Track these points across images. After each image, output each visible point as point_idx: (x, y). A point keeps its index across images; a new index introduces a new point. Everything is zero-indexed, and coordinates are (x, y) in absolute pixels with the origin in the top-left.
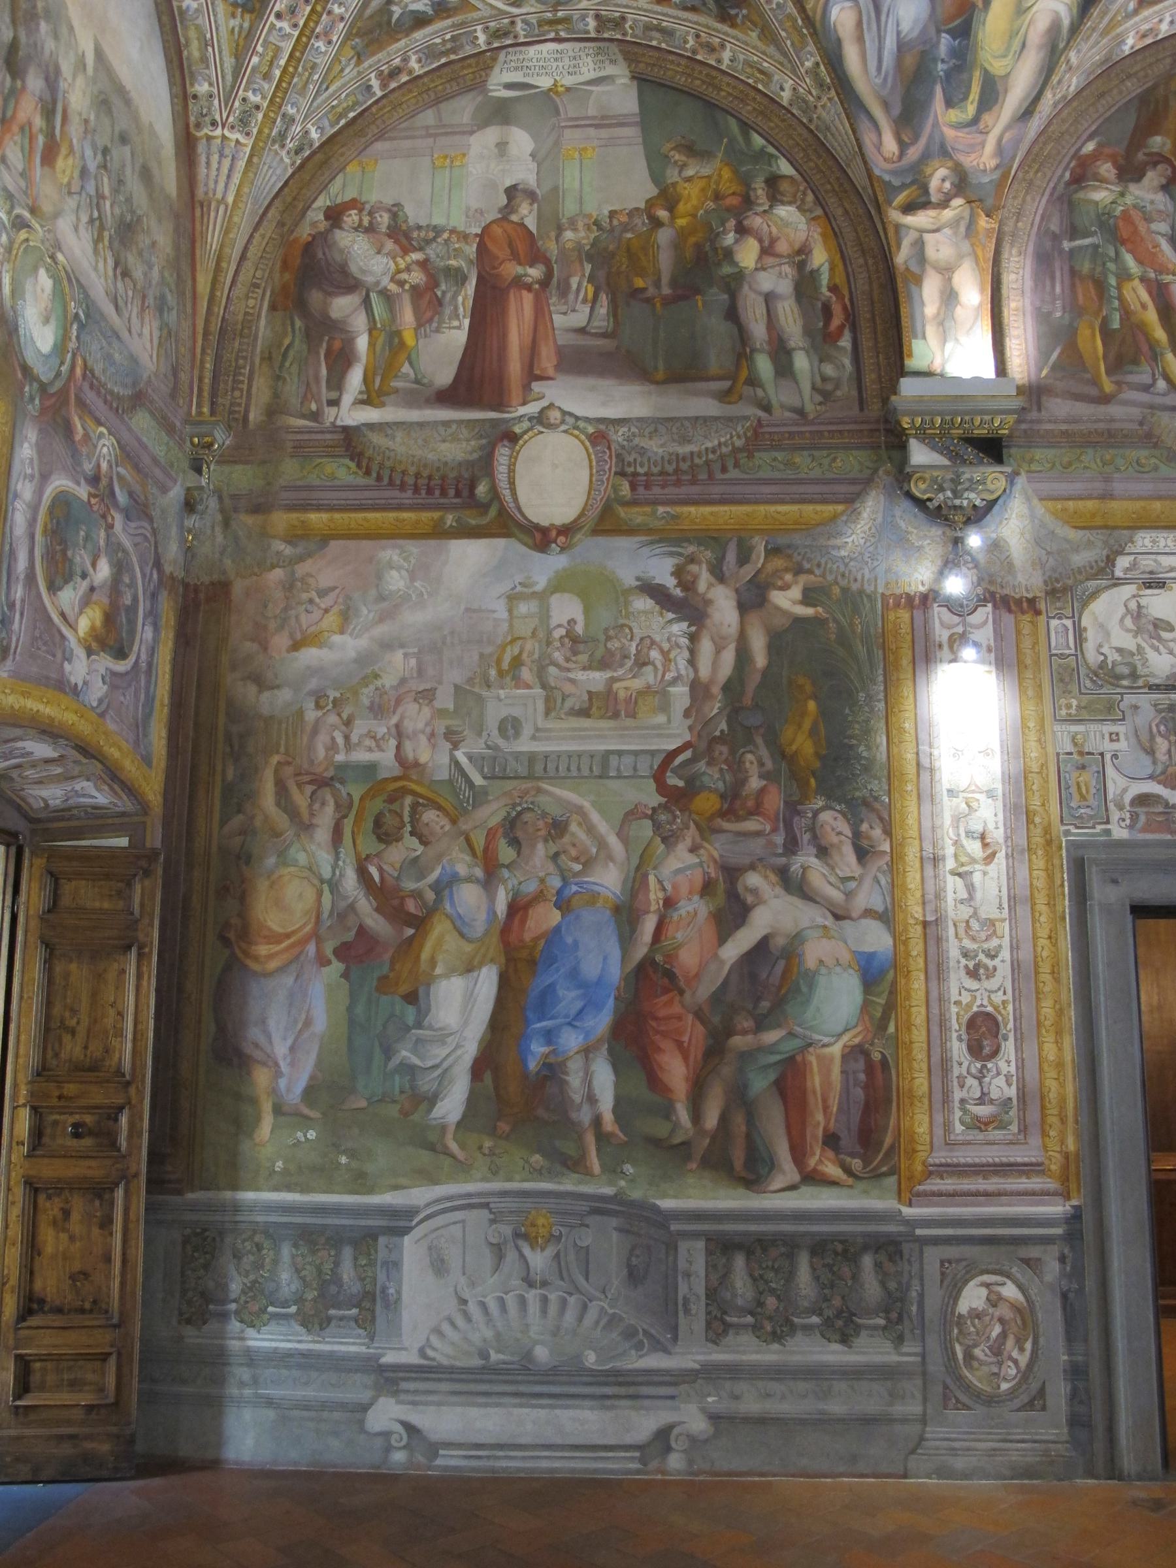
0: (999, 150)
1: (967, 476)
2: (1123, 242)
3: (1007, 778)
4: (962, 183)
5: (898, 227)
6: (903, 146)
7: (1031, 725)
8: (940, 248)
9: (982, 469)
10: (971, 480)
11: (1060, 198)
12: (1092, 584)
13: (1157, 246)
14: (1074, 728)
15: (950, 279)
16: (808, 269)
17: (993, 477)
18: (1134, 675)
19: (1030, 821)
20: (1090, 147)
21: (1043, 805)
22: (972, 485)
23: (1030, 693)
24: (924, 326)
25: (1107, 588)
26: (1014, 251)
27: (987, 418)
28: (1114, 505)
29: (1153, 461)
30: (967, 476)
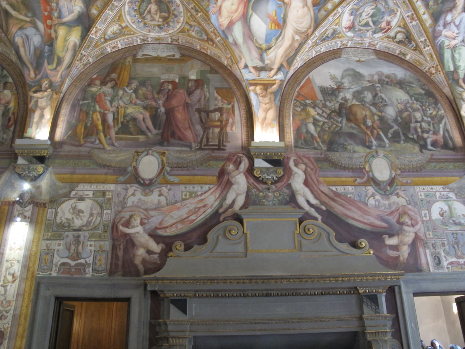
0: (61, 76)
1: (32, 167)
2: (97, 102)
3: (25, 257)
4: (51, 85)
5: (31, 97)
6: (36, 75)
7: (35, 241)
8: (42, 103)
9: (37, 165)
10: (33, 168)
11: (83, 90)
12: (63, 199)
13: (106, 103)
14: (48, 242)
15: (43, 112)
16: (8, 108)
17: (40, 168)
18: (69, 226)
19: (28, 270)
20: (95, 76)
21: (33, 265)
22: (34, 170)
23: (38, 231)
24: (32, 124)
25: (67, 200)
26: (66, 104)
27: (40, 150)
28: (75, 176)
29: (89, 163)
30: (32, 167)
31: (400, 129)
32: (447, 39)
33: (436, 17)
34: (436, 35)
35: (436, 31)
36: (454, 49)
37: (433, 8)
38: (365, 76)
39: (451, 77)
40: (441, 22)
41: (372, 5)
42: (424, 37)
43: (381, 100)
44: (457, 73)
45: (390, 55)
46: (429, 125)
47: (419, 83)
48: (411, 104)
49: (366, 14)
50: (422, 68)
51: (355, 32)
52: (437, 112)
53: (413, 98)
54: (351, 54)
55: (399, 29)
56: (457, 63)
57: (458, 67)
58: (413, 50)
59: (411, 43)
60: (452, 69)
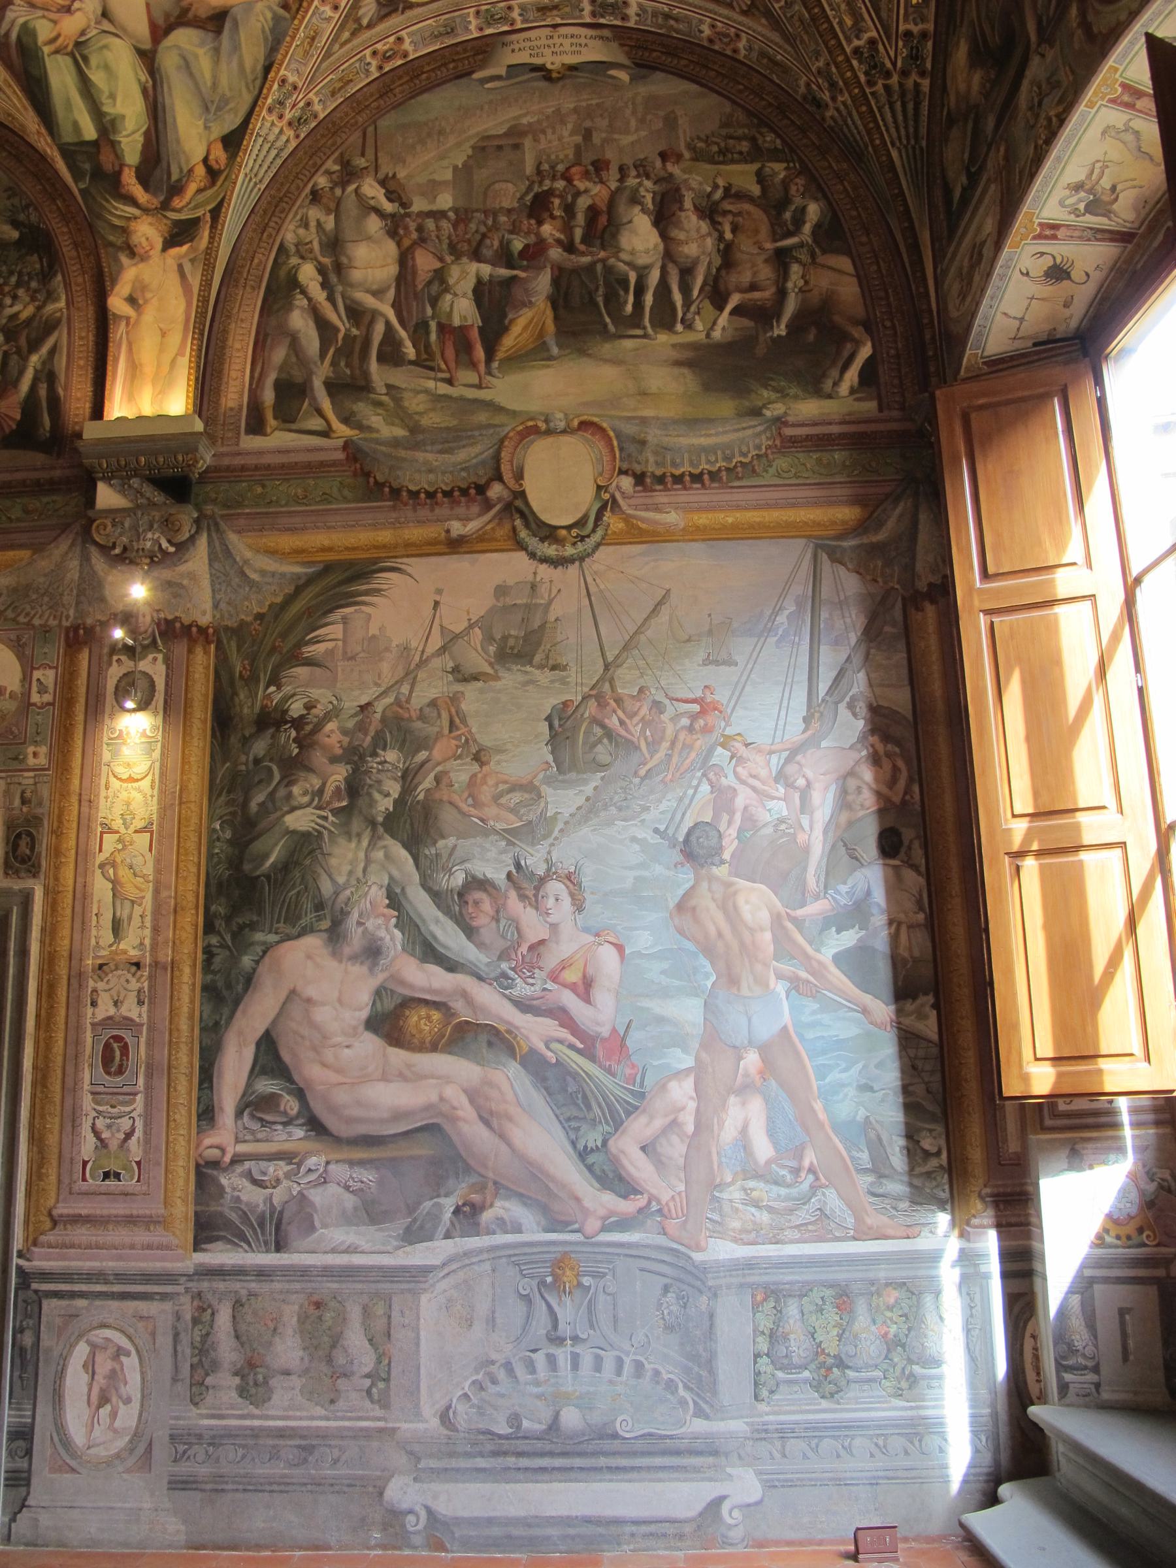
44: (114, 145)
47: (8, 203)
57: (113, 122)
60: (90, 132)
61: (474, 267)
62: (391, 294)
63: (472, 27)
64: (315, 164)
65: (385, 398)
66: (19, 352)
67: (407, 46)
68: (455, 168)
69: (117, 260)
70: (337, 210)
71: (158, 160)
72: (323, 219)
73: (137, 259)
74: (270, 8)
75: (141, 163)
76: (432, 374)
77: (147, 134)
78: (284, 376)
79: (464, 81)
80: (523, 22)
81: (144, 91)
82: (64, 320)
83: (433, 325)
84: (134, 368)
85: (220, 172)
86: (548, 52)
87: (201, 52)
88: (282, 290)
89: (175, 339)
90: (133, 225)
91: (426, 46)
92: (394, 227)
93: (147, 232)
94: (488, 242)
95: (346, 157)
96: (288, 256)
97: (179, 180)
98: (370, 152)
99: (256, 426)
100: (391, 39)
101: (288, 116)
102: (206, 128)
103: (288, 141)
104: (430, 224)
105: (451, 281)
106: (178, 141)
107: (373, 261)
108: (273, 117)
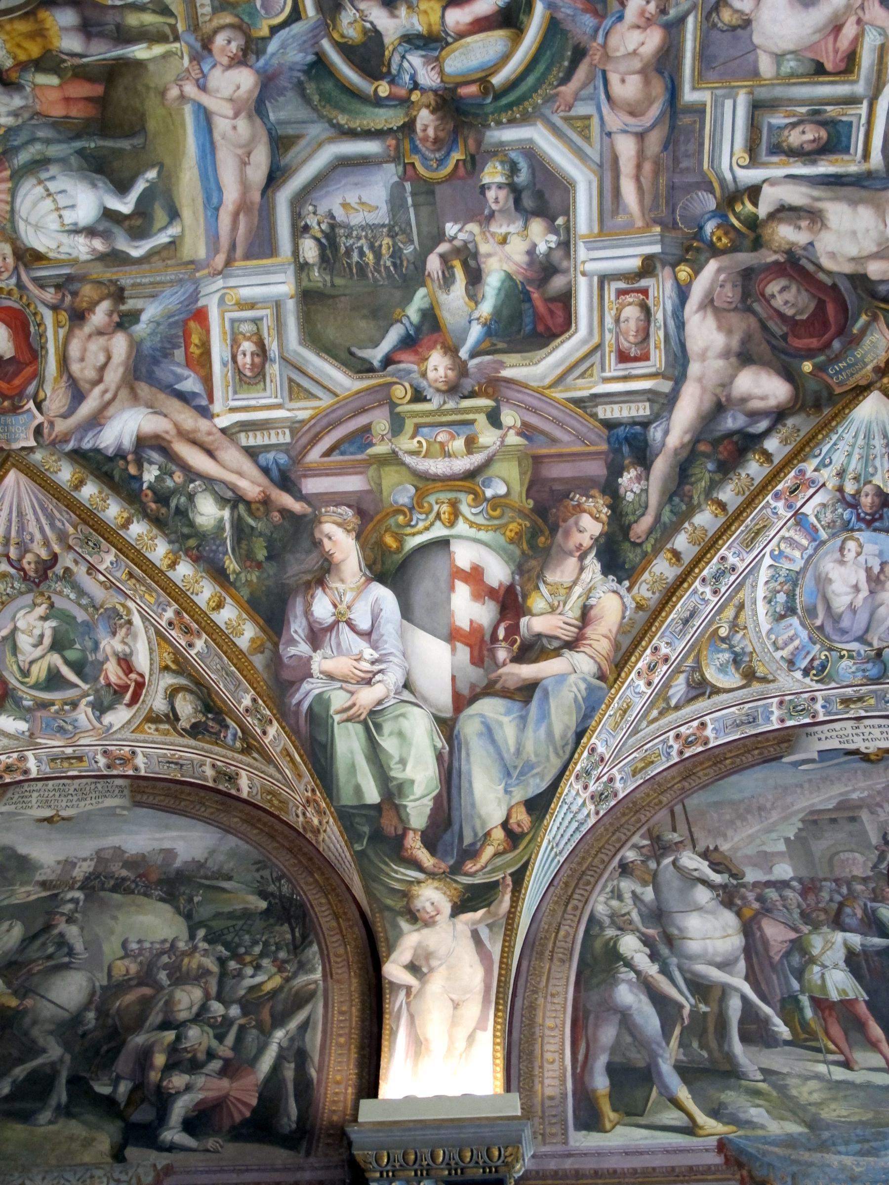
31: (68, 1057)
32: (338, 685)
33: (272, 611)
34: (286, 675)
35: (285, 660)
36: (372, 722)
37: (248, 583)
38: (42, 867)
39: (366, 829)
40: (297, 627)
41: (35, 605)
42: (246, 691)
43: (51, 950)
44: (398, 810)
45: (187, 789)
46: (220, 1038)
47: (257, 876)
48: (184, 954)
49: (31, 640)
50: (290, 819)
51: (23, 713)
52: (287, 980)
53: (201, 933)
54: (34, 800)
55: (169, 680)
56: (396, 773)
57: (401, 787)
58: (243, 751)
59: (227, 727)
60: (372, 795)
61: (839, 937)
62: (742, 965)
63: (774, 718)
64: (619, 840)
65: (763, 1086)
66: (260, 1027)
67: (709, 732)
68: (787, 840)
69: (396, 926)
70: (654, 880)
71: (449, 823)
72: (639, 890)
73: (420, 924)
74: (584, 680)
75: (427, 827)
76: (820, 1056)
77: (437, 799)
78: (617, 1059)
79: (774, 764)
80: (825, 715)
81: (439, 757)
82: (320, 992)
83: (805, 1000)
84: (418, 1044)
85: (523, 835)
86: (855, 738)
87: (506, 720)
88: (599, 964)
89: (473, 1009)
90: (415, 889)
91: (726, 734)
92: (728, 897)
93: (432, 897)
94: (848, 910)
95: (655, 833)
96: (602, 928)
97: (473, 844)
98: (682, 826)
99: (589, 1118)
100: (695, 724)
101: (592, 788)
102: (506, 792)
103: (588, 815)
104: (772, 894)
105: (815, 952)
106: (473, 805)
107: (710, 933)
108: (578, 786)
